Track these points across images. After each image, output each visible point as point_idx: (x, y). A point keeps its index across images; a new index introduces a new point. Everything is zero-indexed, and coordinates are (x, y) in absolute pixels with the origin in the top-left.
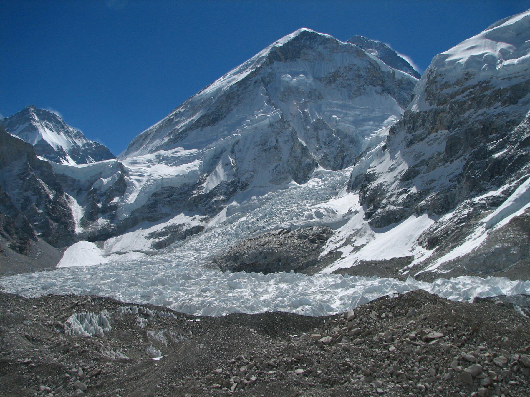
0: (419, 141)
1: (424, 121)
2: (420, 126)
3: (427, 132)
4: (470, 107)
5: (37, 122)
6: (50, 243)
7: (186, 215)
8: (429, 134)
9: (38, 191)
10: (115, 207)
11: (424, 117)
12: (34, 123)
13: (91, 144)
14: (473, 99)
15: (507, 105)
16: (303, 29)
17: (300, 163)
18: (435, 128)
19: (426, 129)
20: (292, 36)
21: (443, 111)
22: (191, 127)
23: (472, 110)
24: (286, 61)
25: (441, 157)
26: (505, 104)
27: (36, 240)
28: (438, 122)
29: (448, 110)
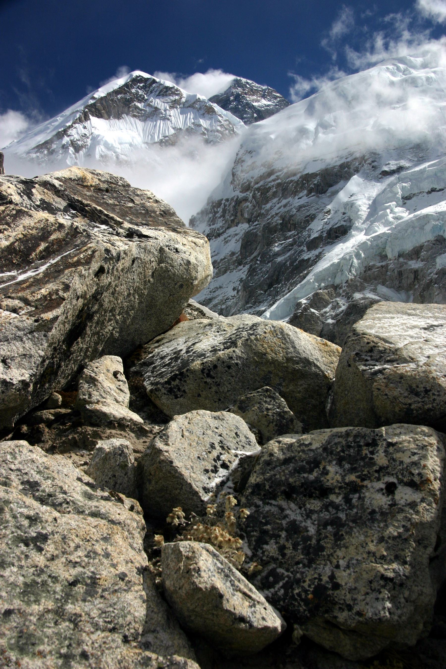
0: (216, 237)
1: (224, 211)
2: (220, 218)
3: (226, 226)
4: (275, 195)
8: (228, 228)
11: (225, 206)
15: (313, 194)
16: (137, 73)
18: (236, 221)
19: (226, 222)
21: (245, 199)
23: (275, 200)
24: (109, 118)
25: (234, 258)
26: (311, 193)
28: (239, 214)
29: (250, 198)
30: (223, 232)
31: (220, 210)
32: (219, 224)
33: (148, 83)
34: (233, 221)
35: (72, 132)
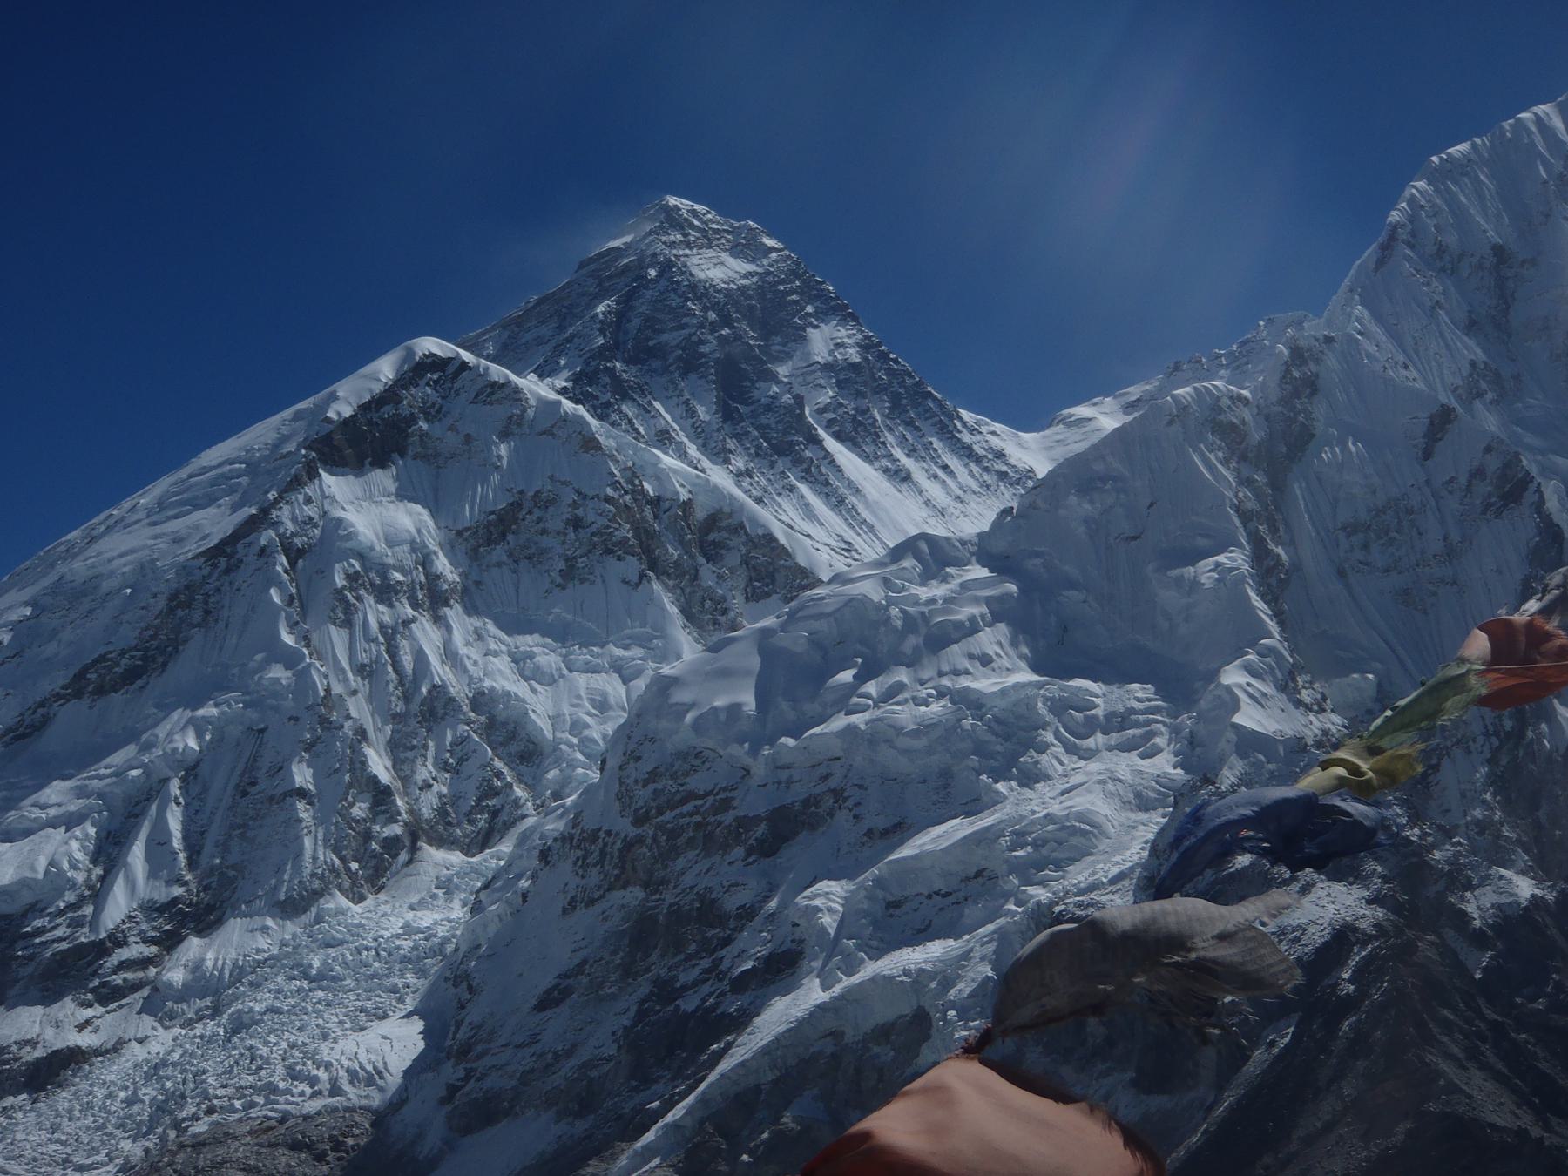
1: (603, 854)
4: (691, 843)
11: (605, 845)
14: (698, 825)
20: (386, 368)
21: (640, 840)
23: (692, 854)
28: (629, 866)
29: (649, 841)
30: (602, 897)
31: (595, 849)
32: (594, 876)
33: (451, 369)
34: (617, 877)
35: (284, 514)
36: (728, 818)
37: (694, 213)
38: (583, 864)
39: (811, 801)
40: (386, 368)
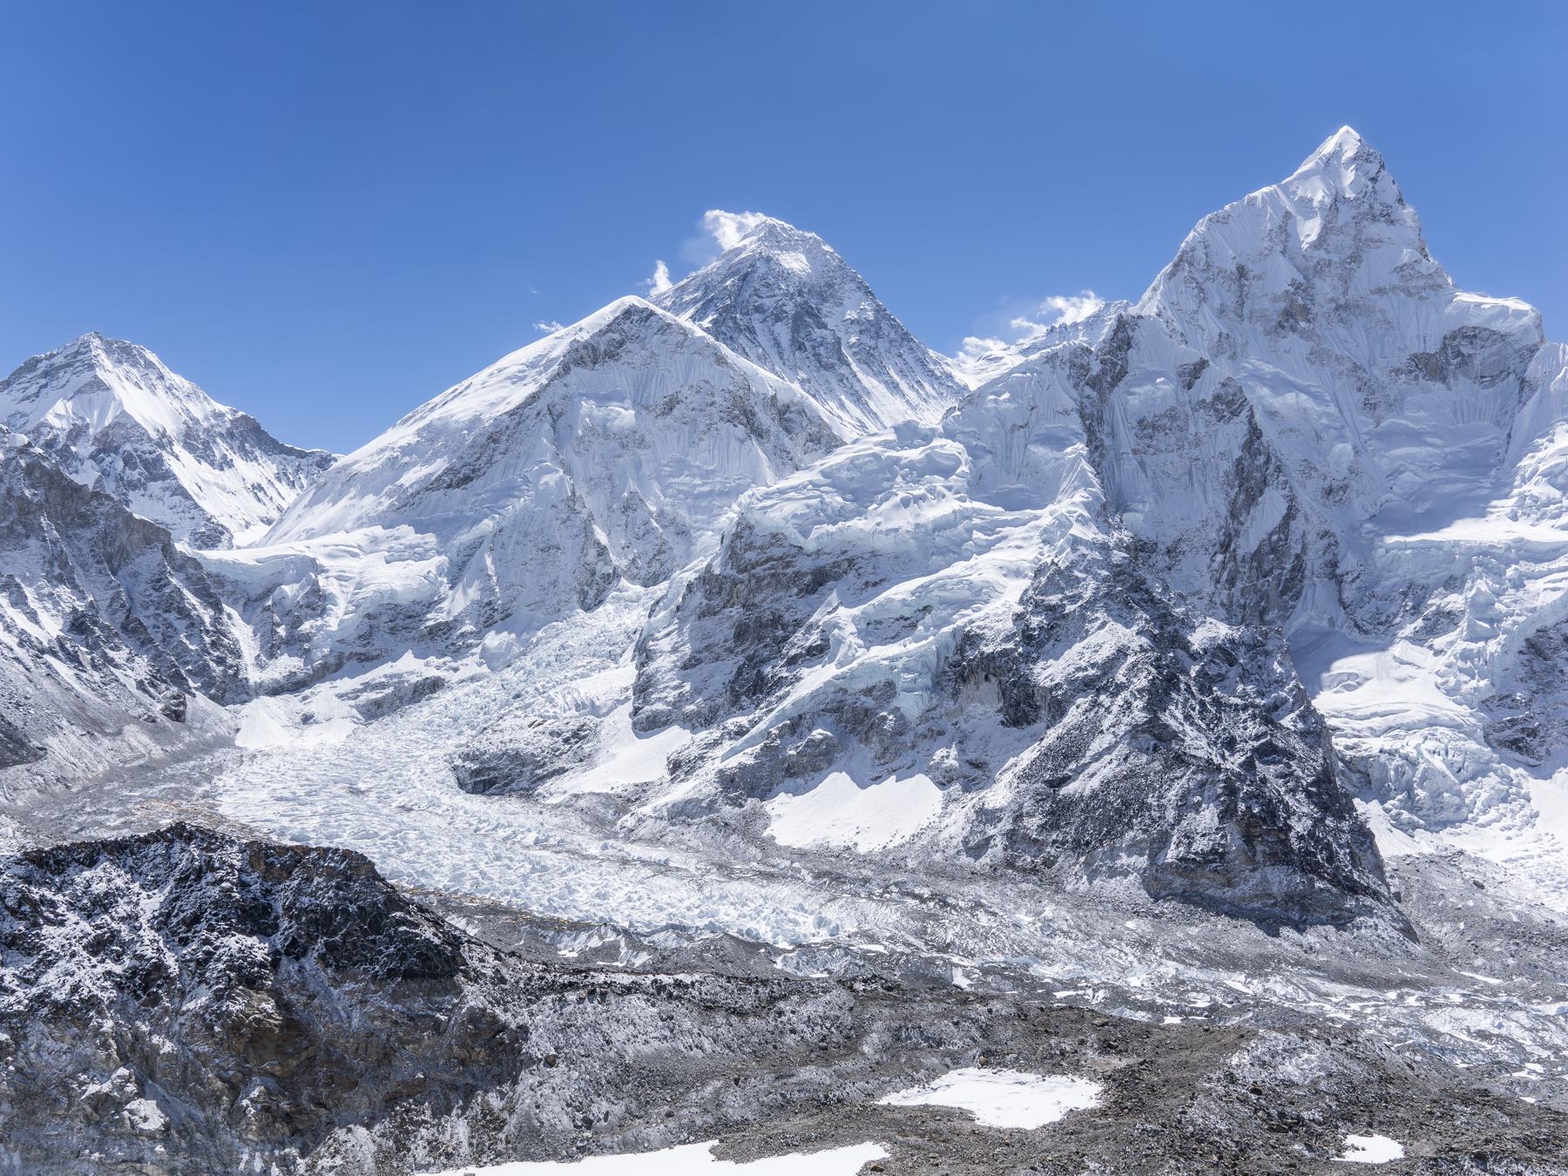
5: (109, 371)
6: (212, 698)
7: (416, 657)
9: (184, 613)
10: (308, 638)
12: (100, 373)
13: (222, 415)
17: (593, 573)
22: (431, 485)
27: (194, 696)
36: (790, 571)
37: (783, 228)
38: (709, 595)
39: (836, 565)
40: (607, 313)
